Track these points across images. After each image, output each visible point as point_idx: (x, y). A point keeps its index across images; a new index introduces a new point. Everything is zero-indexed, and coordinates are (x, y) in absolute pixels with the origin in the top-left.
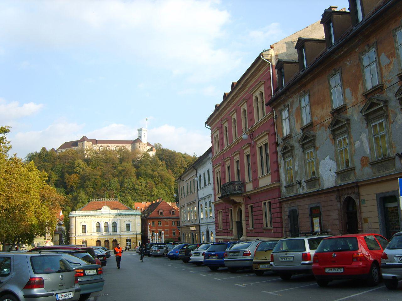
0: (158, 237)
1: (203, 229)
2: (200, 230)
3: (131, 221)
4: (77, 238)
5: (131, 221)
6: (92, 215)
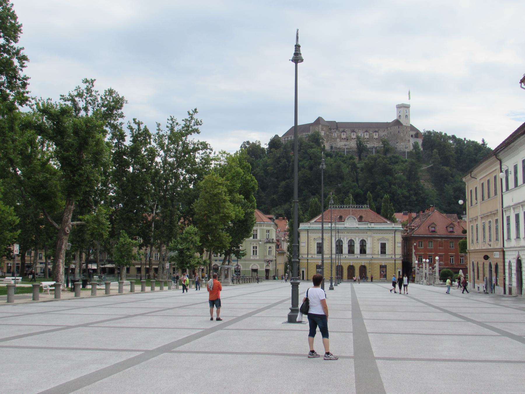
0: (428, 265)
1: (511, 258)
2: (504, 259)
3: (388, 240)
5: (388, 240)
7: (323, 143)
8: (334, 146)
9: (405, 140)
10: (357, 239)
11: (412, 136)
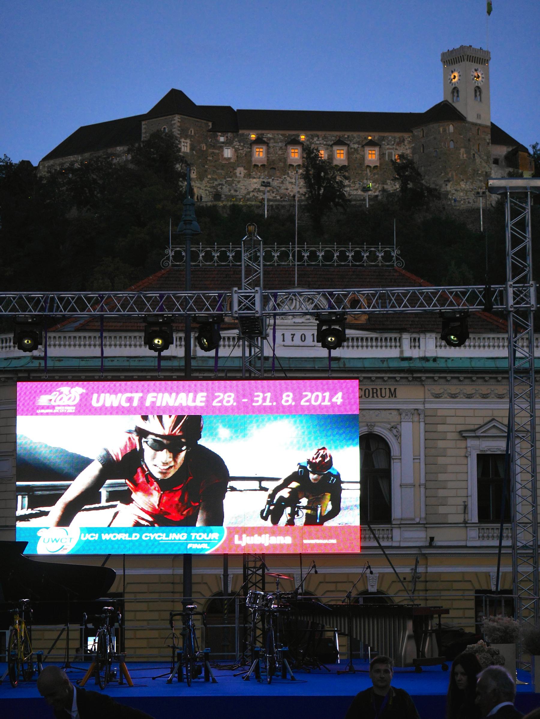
7: (185, 176)
8: (225, 189)
9: (475, 171)
11: (496, 162)
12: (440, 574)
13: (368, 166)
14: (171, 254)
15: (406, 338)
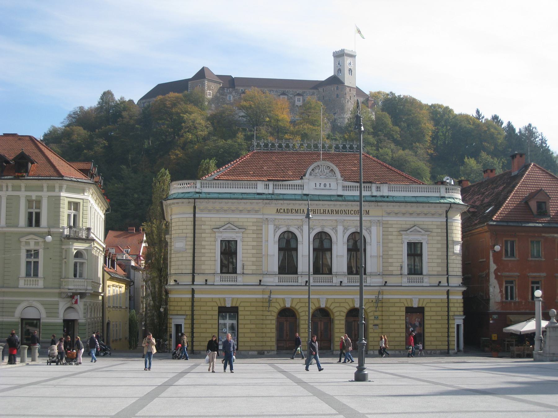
4: (196, 296)
6: (264, 196)
10: (340, 229)
12: (389, 299)
13: (297, 106)
14: (255, 144)
15: (374, 186)
